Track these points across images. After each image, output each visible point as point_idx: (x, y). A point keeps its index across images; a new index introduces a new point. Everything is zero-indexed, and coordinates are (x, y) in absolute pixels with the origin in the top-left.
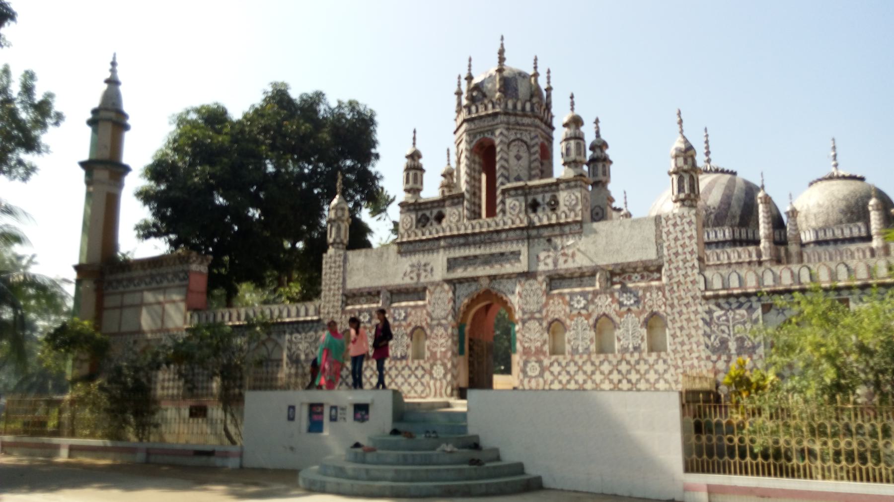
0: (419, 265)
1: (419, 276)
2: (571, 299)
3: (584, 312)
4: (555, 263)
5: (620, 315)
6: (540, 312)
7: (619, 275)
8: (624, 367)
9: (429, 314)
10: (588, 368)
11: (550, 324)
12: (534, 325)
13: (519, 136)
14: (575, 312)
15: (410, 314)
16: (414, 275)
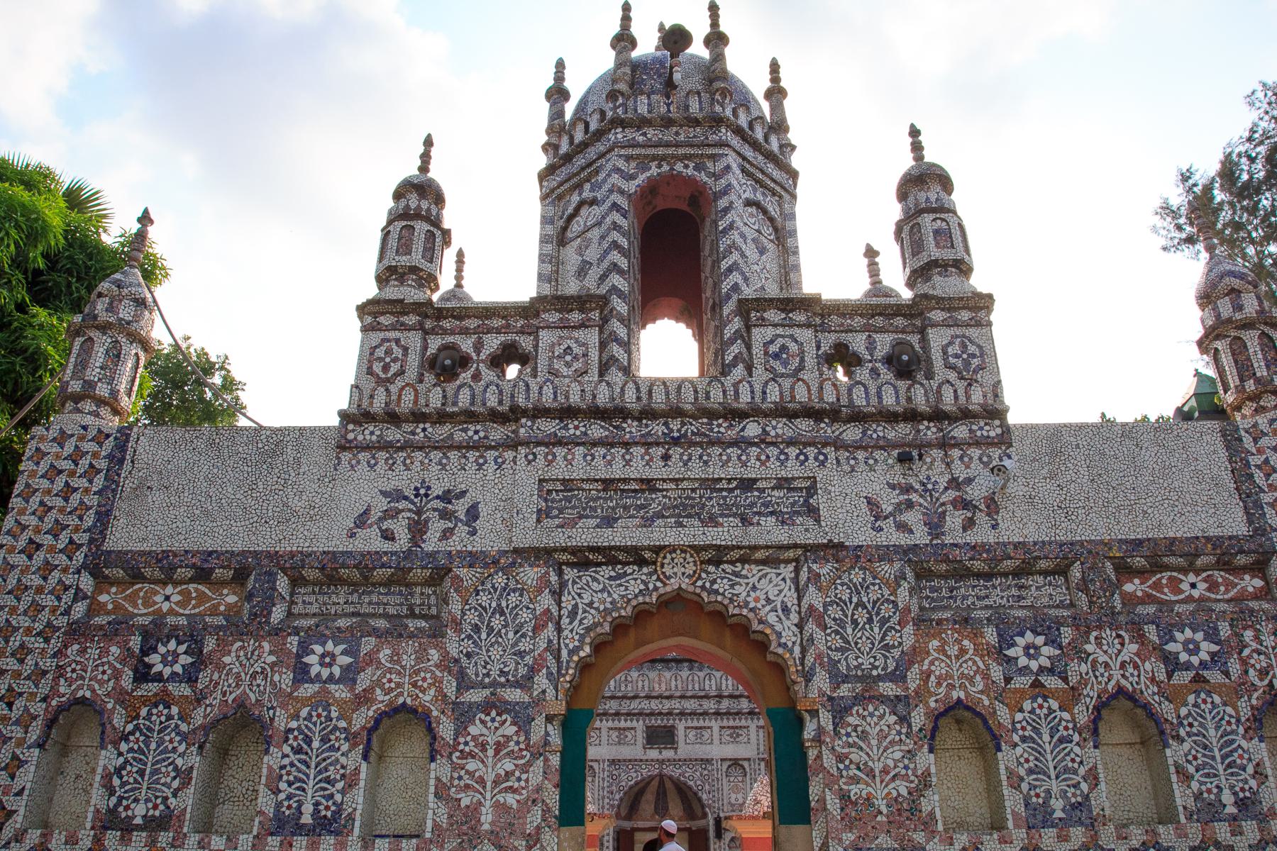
0: (422, 492)
1: (418, 529)
2: (1006, 641)
3: (1052, 682)
4: (935, 526)
5: (1175, 696)
6: (898, 676)
7: (1142, 573)
9: (449, 663)
11: (937, 718)
13: (760, 197)
14: (1022, 682)
15: (372, 659)
16: (400, 528)
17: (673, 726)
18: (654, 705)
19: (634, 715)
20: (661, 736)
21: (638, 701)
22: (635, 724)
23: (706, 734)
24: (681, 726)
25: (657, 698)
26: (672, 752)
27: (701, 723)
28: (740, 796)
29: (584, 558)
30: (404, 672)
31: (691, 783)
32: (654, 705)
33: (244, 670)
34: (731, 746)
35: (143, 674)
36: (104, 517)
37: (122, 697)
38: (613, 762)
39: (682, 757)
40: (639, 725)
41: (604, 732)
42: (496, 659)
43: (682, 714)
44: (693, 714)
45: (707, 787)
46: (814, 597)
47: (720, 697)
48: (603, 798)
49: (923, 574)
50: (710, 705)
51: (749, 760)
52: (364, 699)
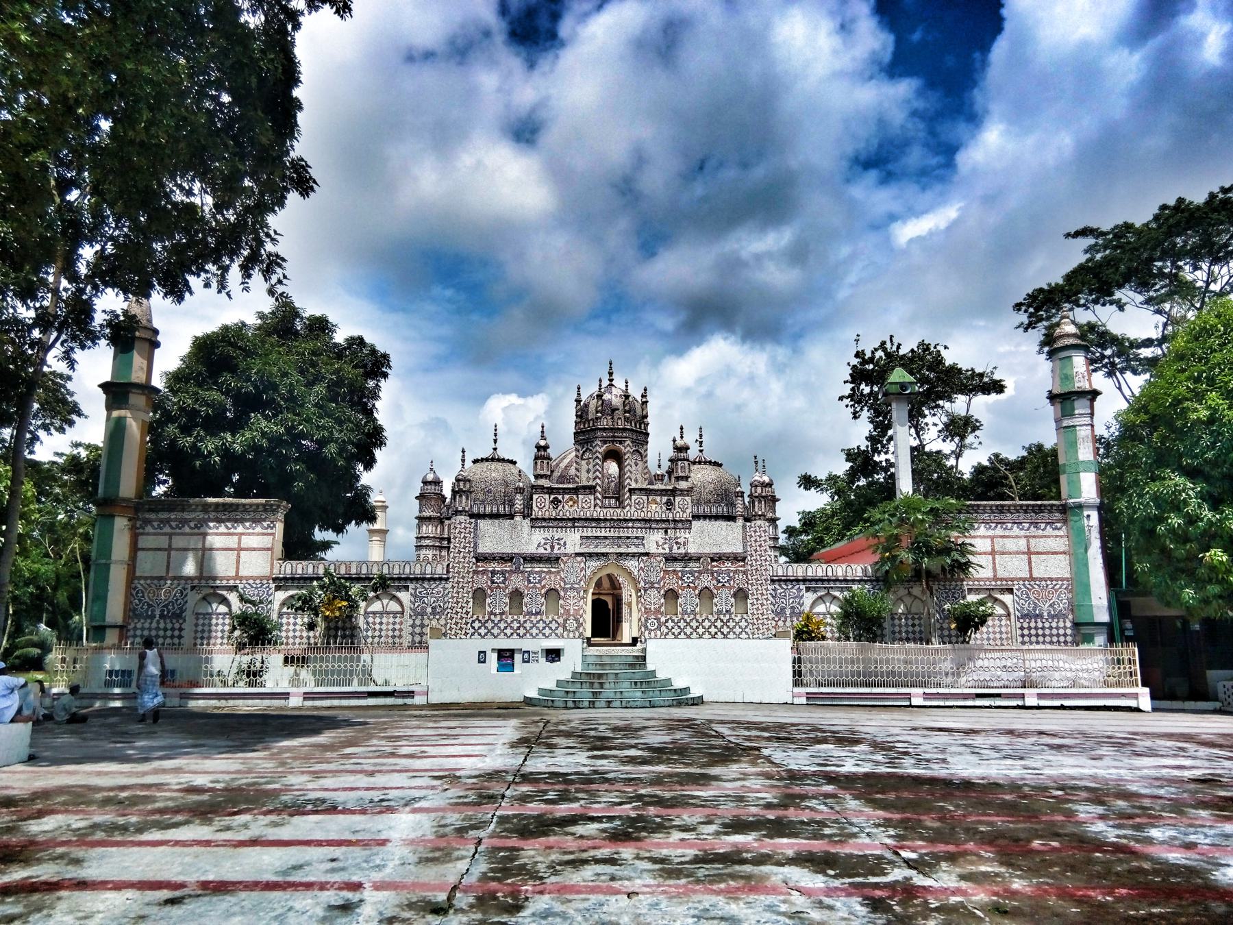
0: (553, 538)
1: (552, 548)
4: (671, 549)
5: (718, 588)
6: (659, 583)
8: (719, 624)
9: (562, 579)
10: (694, 624)
12: (653, 592)
16: (548, 547)
29: (591, 555)
30: (552, 581)
33: (516, 581)
35: (493, 582)
36: (476, 544)
37: (490, 587)
42: (572, 579)
46: (642, 565)
49: (667, 560)
52: (543, 587)
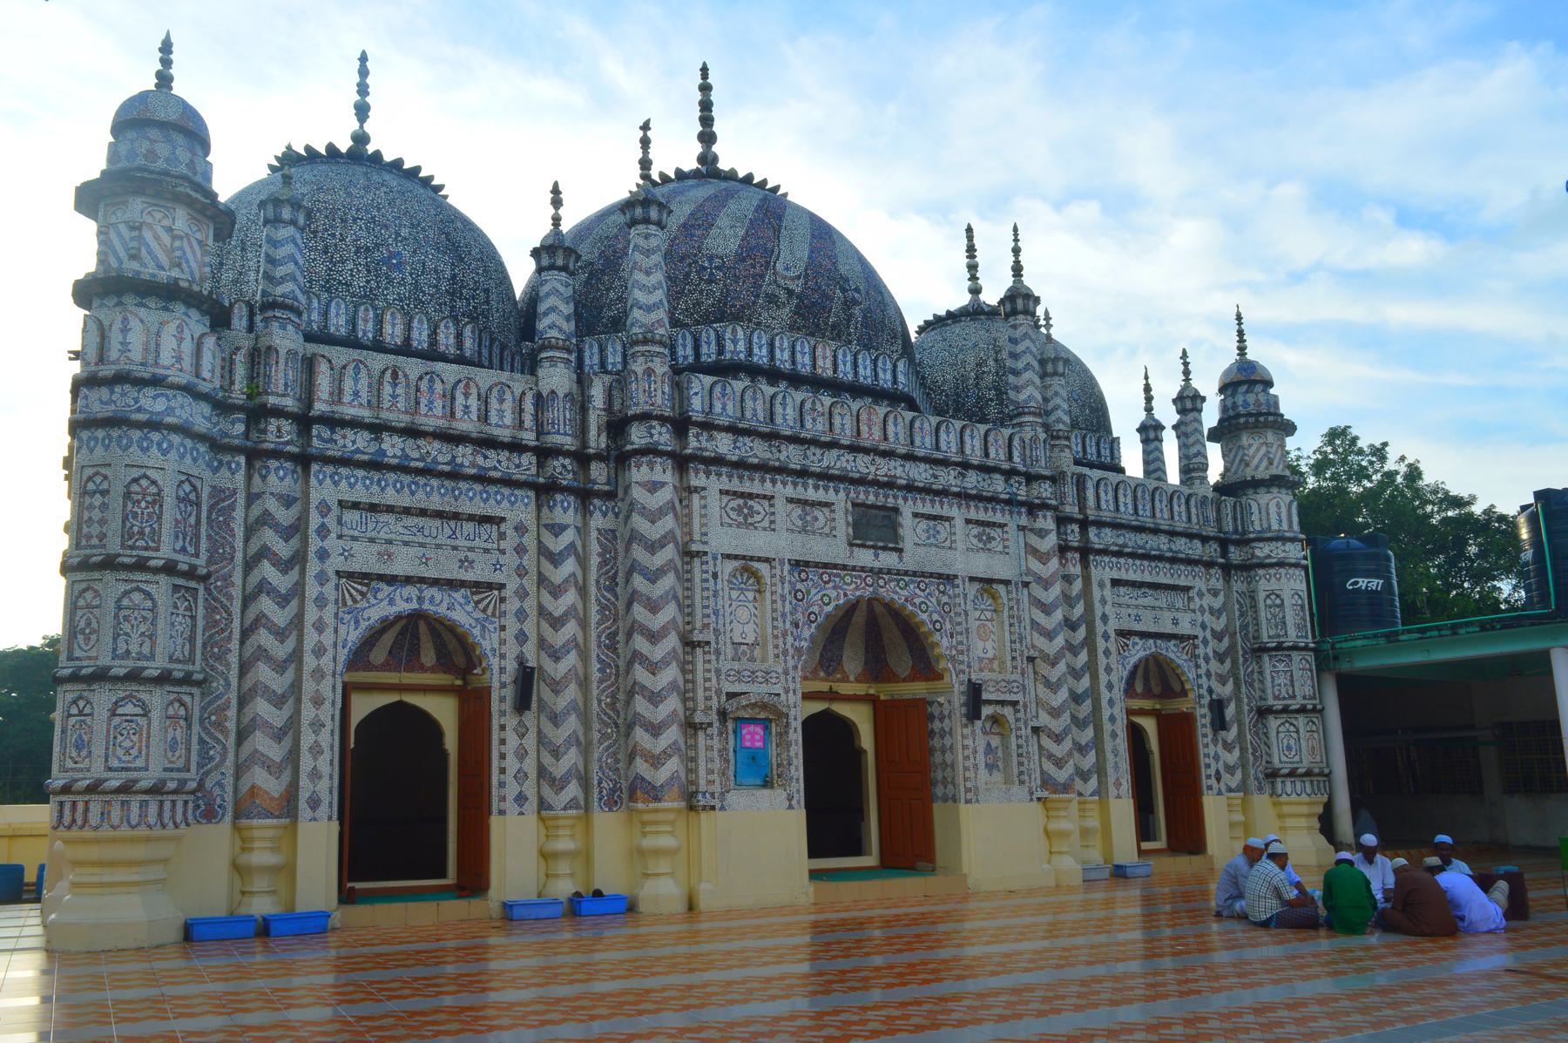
17: (896, 510)
18: (862, 465)
19: (831, 478)
20: (874, 526)
21: (835, 452)
22: (831, 496)
23: (943, 528)
24: (907, 509)
25: (866, 451)
26: (895, 555)
27: (937, 510)
28: (989, 645)
31: (924, 616)
32: (862, 465)
34: (981, 554)
38: (798, 565)
39: (911, 568)
40: (839, 498)
41: (780, 503)
43: (910, 488)
44: (927, 490)
45: (948, 626)
47: (966, 466)
48: (785, 634)
50: (948, 478)
51: (1007, 583)
